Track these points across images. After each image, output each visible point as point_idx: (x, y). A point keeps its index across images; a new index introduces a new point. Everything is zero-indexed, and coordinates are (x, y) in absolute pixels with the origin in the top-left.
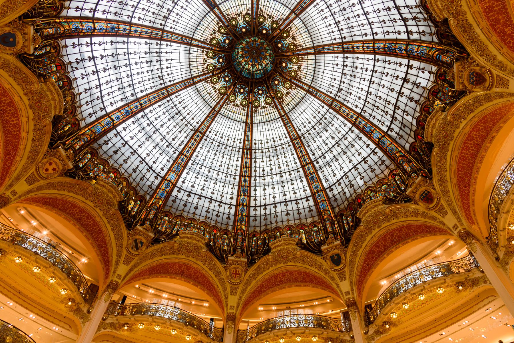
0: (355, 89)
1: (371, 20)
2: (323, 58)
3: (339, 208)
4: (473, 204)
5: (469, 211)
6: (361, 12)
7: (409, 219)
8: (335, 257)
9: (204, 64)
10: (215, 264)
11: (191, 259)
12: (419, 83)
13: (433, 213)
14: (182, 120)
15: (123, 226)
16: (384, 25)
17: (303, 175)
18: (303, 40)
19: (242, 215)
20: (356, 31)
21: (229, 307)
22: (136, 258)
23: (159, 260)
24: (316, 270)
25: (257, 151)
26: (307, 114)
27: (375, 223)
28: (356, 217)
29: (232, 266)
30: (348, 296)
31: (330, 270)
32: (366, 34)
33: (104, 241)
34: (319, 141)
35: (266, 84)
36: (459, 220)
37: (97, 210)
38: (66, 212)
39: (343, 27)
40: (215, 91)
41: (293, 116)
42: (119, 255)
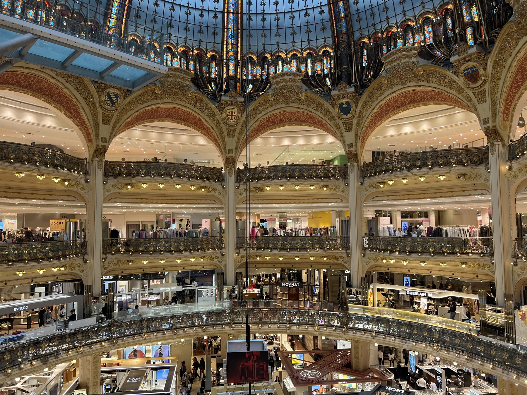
3: (361, 33)
4: (519, 98)
5: (510, 105)
7: (441, 87)
8: (345, 106)
10: (207, 105)
11: (177, 102)
13: (470, 93)
24: (322, 116)
27: (401, 79)
28: (380, 61)
29: (227, 108)
30: (351, 149)
31: (336, 118)
36: (494, 115)
37: (47, 71)
38: (8, 83)
42: (95, 116)
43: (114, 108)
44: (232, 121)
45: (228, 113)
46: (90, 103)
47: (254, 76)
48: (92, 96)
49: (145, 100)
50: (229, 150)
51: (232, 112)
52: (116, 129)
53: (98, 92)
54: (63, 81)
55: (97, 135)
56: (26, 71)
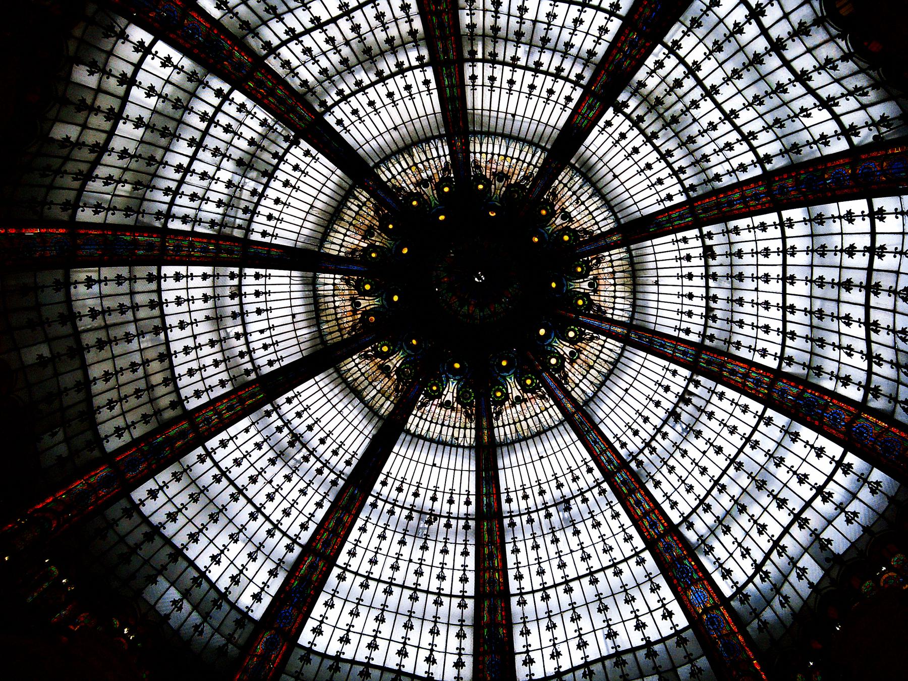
0: (686, 462)
1: (790, 327)
2: (641, 361)
6: (777, 299)
9: (364, 238)
12: (855, 514)
14: (238, 336)
16: (818, 350)
17: (469, 621)
18: (614, 301)
20: (744, 335)
25: (380, 504)
26: (544, 471)
32: (764, 353)
34: (548, 549)
39: (719, 314)
40: (354, 312)
41: (505, 461)
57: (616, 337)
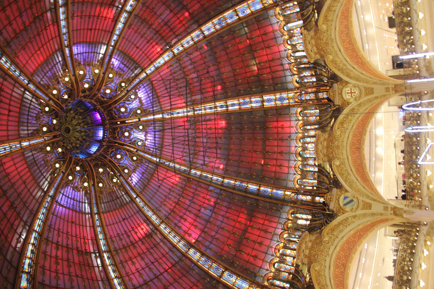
15: (335, 222)
19: (276, 100)
21: (386, 93)
22: (361, 198)
23: (354, 177)
33: (354, 236)
35: (110, 105)
38: (343, 281)
42: (365, 215)
43: (355, 200)
44: (356, 92)
45: (350, 97)
46: (353, 220)
47: (312, 75)
48: (347, 218)
49: (346, 173)
50: (386, 91)
51: (348, 93)
52: (375, 198)
53: (343, 213)
54: (337, 240)
55: (381, 214)
56: (332, 268)
57: (71, 51)
